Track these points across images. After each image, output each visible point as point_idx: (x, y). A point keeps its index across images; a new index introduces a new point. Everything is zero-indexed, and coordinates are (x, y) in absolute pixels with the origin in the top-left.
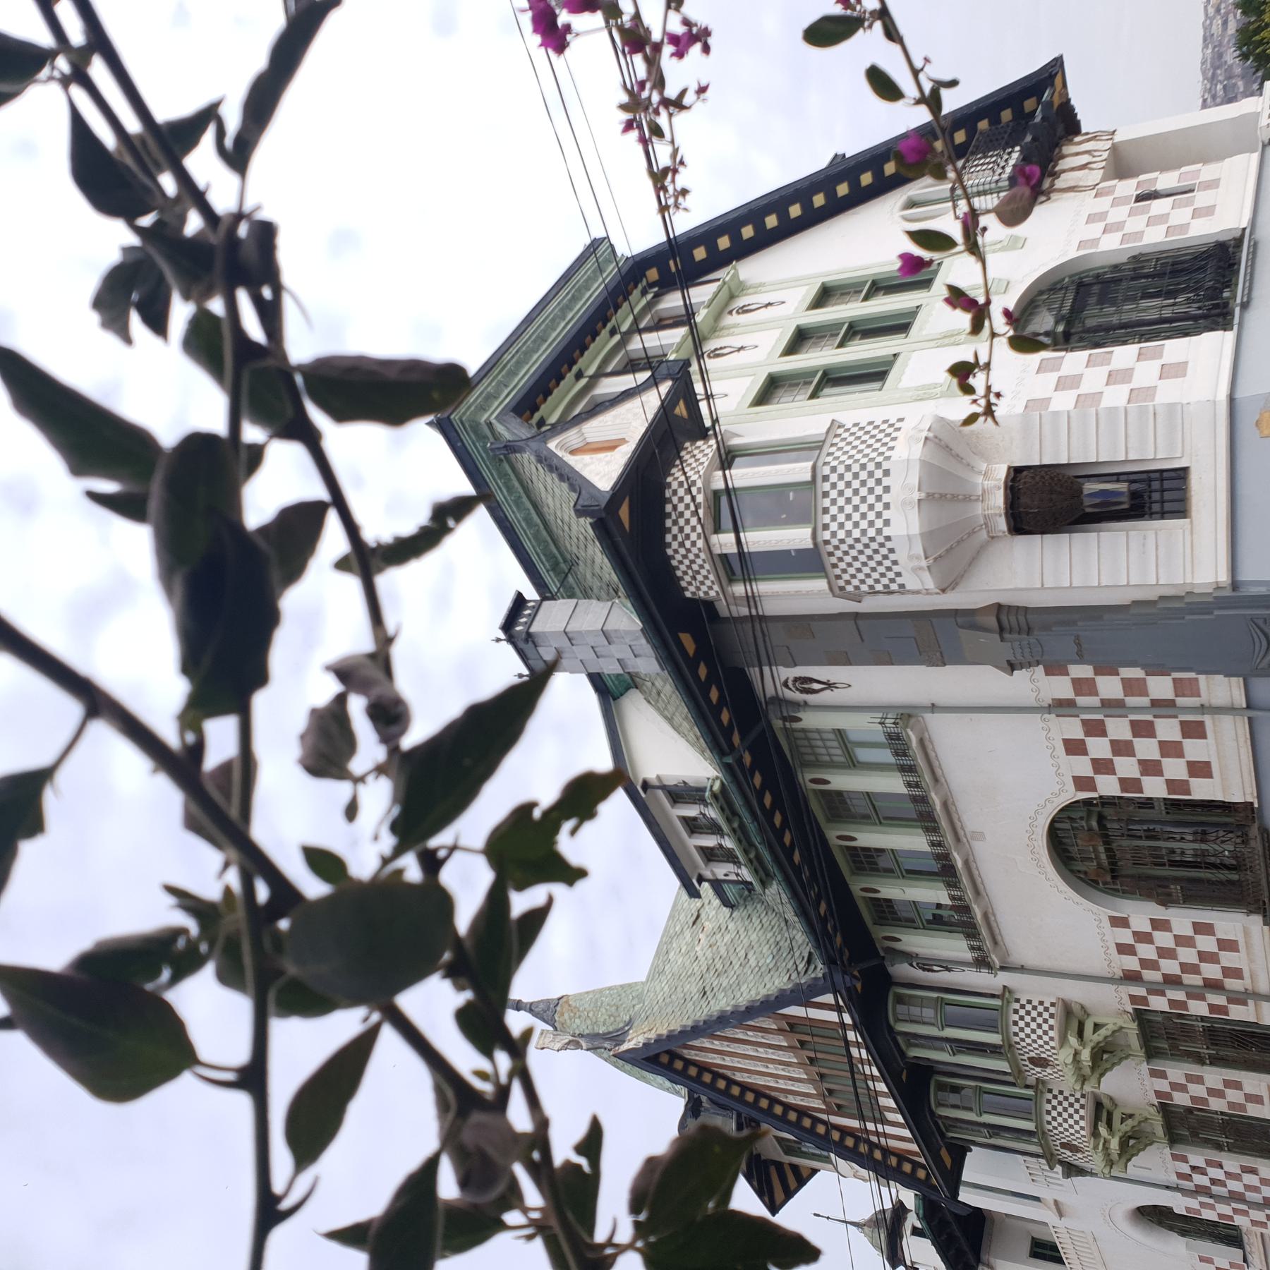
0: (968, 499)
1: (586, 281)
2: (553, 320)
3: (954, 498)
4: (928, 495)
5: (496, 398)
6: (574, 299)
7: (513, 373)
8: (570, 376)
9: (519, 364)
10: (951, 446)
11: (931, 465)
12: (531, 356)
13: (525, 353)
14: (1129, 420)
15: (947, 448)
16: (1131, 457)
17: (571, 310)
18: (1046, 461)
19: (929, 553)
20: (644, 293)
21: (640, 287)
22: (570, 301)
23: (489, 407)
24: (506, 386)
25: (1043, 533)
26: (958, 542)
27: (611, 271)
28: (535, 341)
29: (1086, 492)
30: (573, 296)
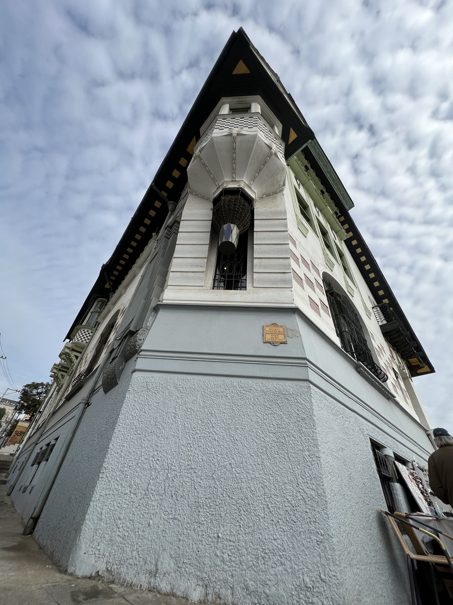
0: (234, 171)
1: (340, 189)
3: (234, 160)
4: (234, 138)
10: (267, 165)
11: (254, 142)
13: (314, 147)
14: (280, 260)
15: (265, 163)
16: (255, 261)
18: (255, 222)
19: (203, 152)
21: (338, 212)
22: (333, 178)
25: (213, 220)
26: (209, 172)
28: (319, 154)
29: (232, 225)
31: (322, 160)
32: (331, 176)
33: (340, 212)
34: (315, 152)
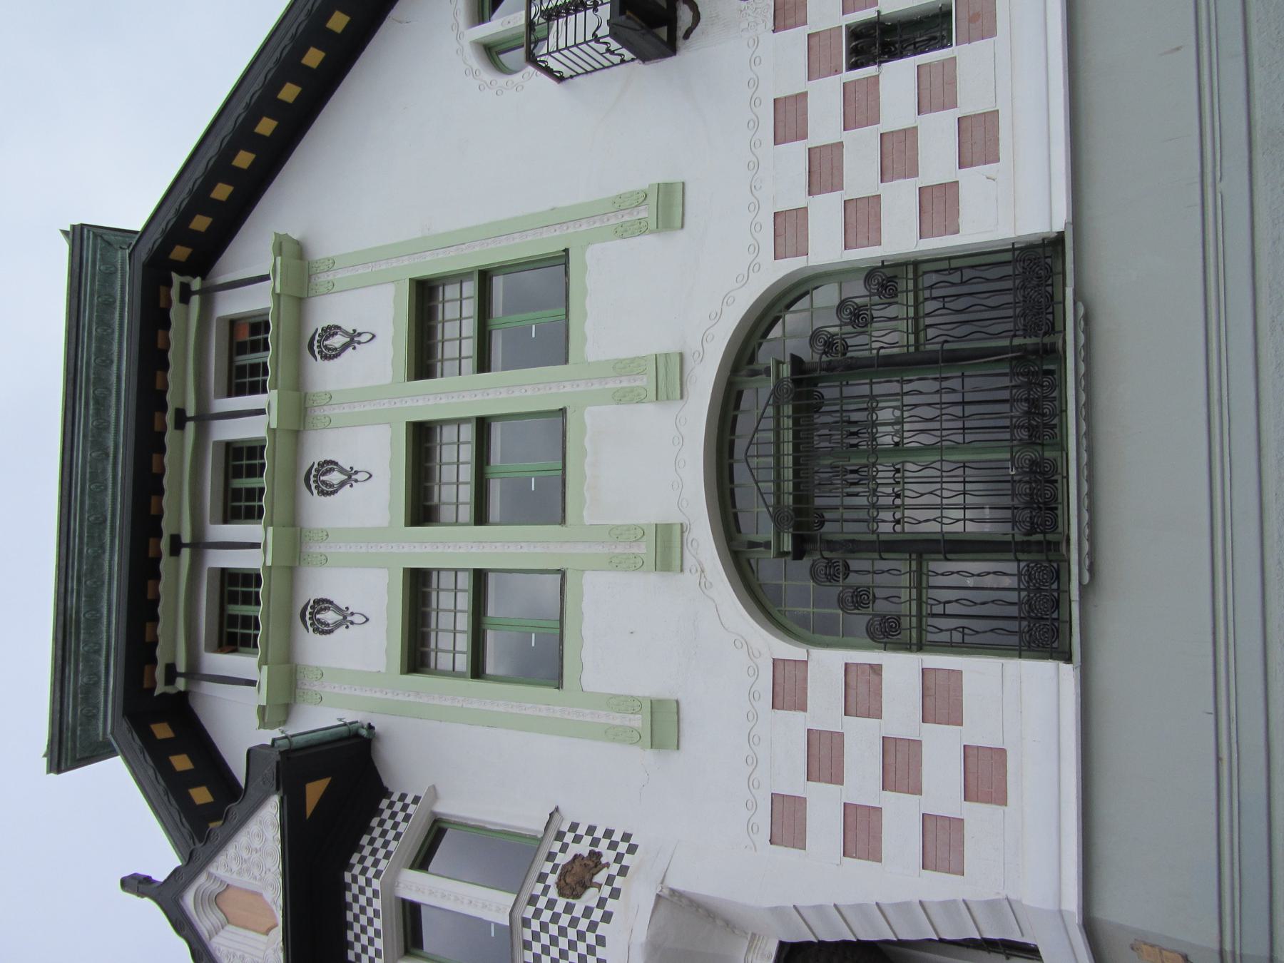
2: (94, 477)
5: (96, 684)
6: (101, 403)
7: (94, 622)
8: (165, 564)
9: (93, 599)
12: (101, 567)
13: (91, 572)
17: (107, 429)
20: (186, 295)
21: (175, 293)
22: (98, 413)
23: (96, 707)
24: (98, 652)
27: (125, 289)
28: (91, 537)
30: (97, 402)
31: (93, 506)
32: (101, 429)
33: (169, 284)
34: (97, 557)
